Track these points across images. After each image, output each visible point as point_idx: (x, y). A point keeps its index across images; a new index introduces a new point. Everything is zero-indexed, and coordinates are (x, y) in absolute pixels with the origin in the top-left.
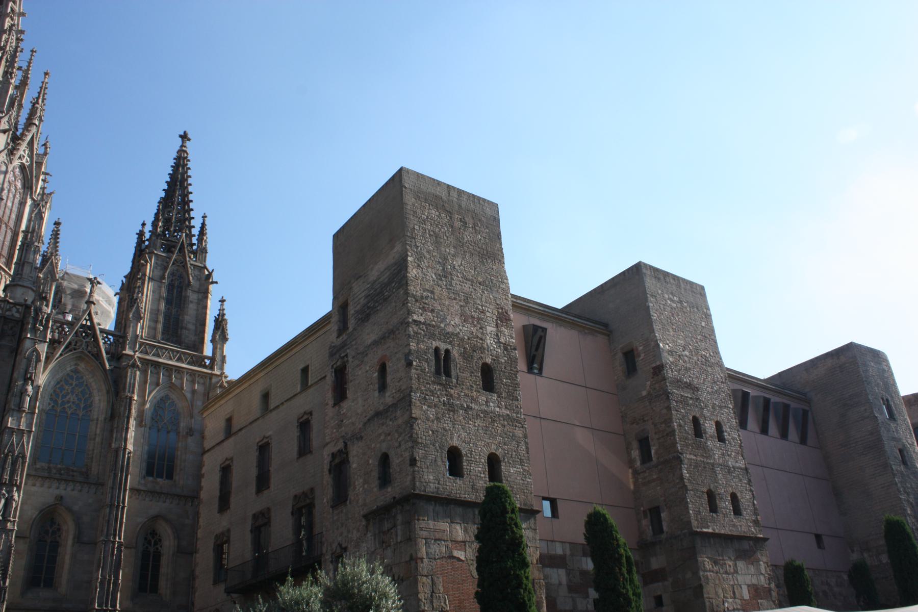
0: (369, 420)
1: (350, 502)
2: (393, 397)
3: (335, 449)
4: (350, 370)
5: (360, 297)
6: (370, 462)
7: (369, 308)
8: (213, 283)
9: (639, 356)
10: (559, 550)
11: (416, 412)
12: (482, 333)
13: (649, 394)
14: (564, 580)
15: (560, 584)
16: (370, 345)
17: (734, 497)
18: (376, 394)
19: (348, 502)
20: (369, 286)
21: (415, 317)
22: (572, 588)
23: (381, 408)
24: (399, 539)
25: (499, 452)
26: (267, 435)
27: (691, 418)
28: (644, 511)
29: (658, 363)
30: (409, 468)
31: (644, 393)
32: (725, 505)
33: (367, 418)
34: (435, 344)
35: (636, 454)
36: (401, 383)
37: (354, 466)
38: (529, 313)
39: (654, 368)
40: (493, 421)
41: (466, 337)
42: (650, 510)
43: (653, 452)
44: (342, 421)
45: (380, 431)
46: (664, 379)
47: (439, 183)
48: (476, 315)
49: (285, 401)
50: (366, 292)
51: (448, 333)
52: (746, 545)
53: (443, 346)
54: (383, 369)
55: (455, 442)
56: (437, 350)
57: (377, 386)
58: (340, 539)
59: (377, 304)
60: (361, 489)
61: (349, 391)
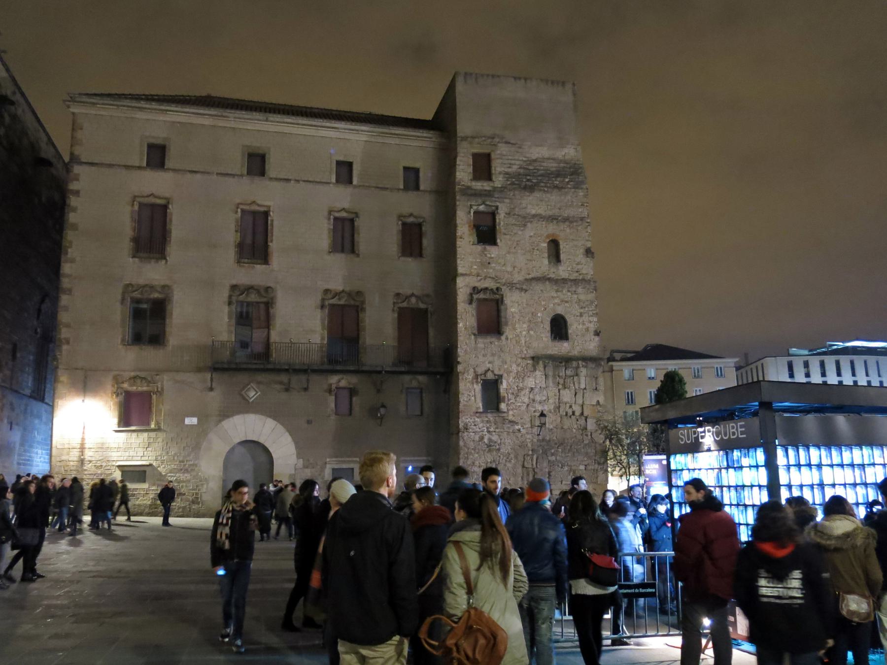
2: (570, 274)
3: (482, 285)
4: (502, 223)
5: (513, 162)
6: (539, 315)
7: (528, 180)
19: (503, 338)
20: (524, 159)
23: (552, 276)
24: (583, 386)
30: (593, 337)
33: (530, 276)
36: (580, 267)
44: (489, 263)
49: (304, 181)
50: (521, 163)
54: (554, 246)
59: (542, 184)
60: (524, 333)
61: (501, 241)
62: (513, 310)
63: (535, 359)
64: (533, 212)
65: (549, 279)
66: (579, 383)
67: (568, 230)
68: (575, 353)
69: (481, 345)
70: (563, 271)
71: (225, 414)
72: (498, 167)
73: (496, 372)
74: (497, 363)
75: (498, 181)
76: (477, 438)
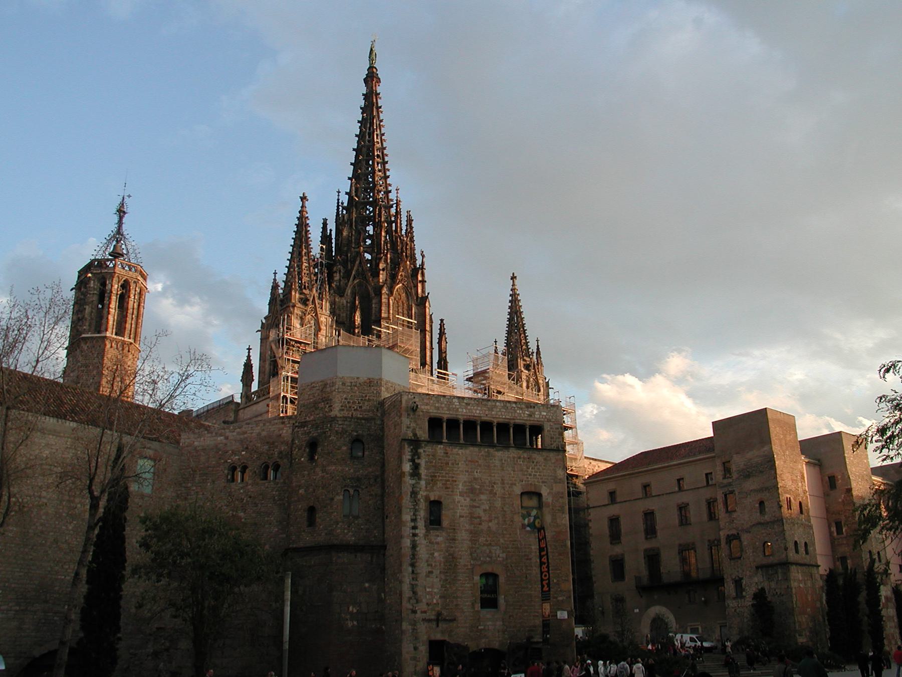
0: (754, 525)
1: (744, 559)
3: (730, 533)
7: (748, 472)
8: (551, 388)
9: (838, 481)
11: (785, 528)
13: (843, 501)
16: (751, 491)
17: (879, 553)
18: (758, 514)
19: (742, 558)
23: (762, 521)
25: (807, 542)
26: (651, 508)
28: (838, 558)
29: (849, 487)
31: (840, 500)
35: (834, 529)
37: (745, 543)
39: (847, 489)
42: (841, 558)
43: (844, 530)
45: (763, 531)
46: (852, 496)
54: (762, 503)
57: (758, 511)
58: (737, 573)
62: (745, 543)
63: (757, 568)
64: (751, 489)
65: (759, 524)
66: (778, 577)
67: (768, 494)
68: (776, 561)
69: (732, 564)
70: (767, 518)
71: (648, 607)
72: (734, 468)
73: (740, 576)
74: (740, 571)
75: (735, 475)
76: (733, 610)
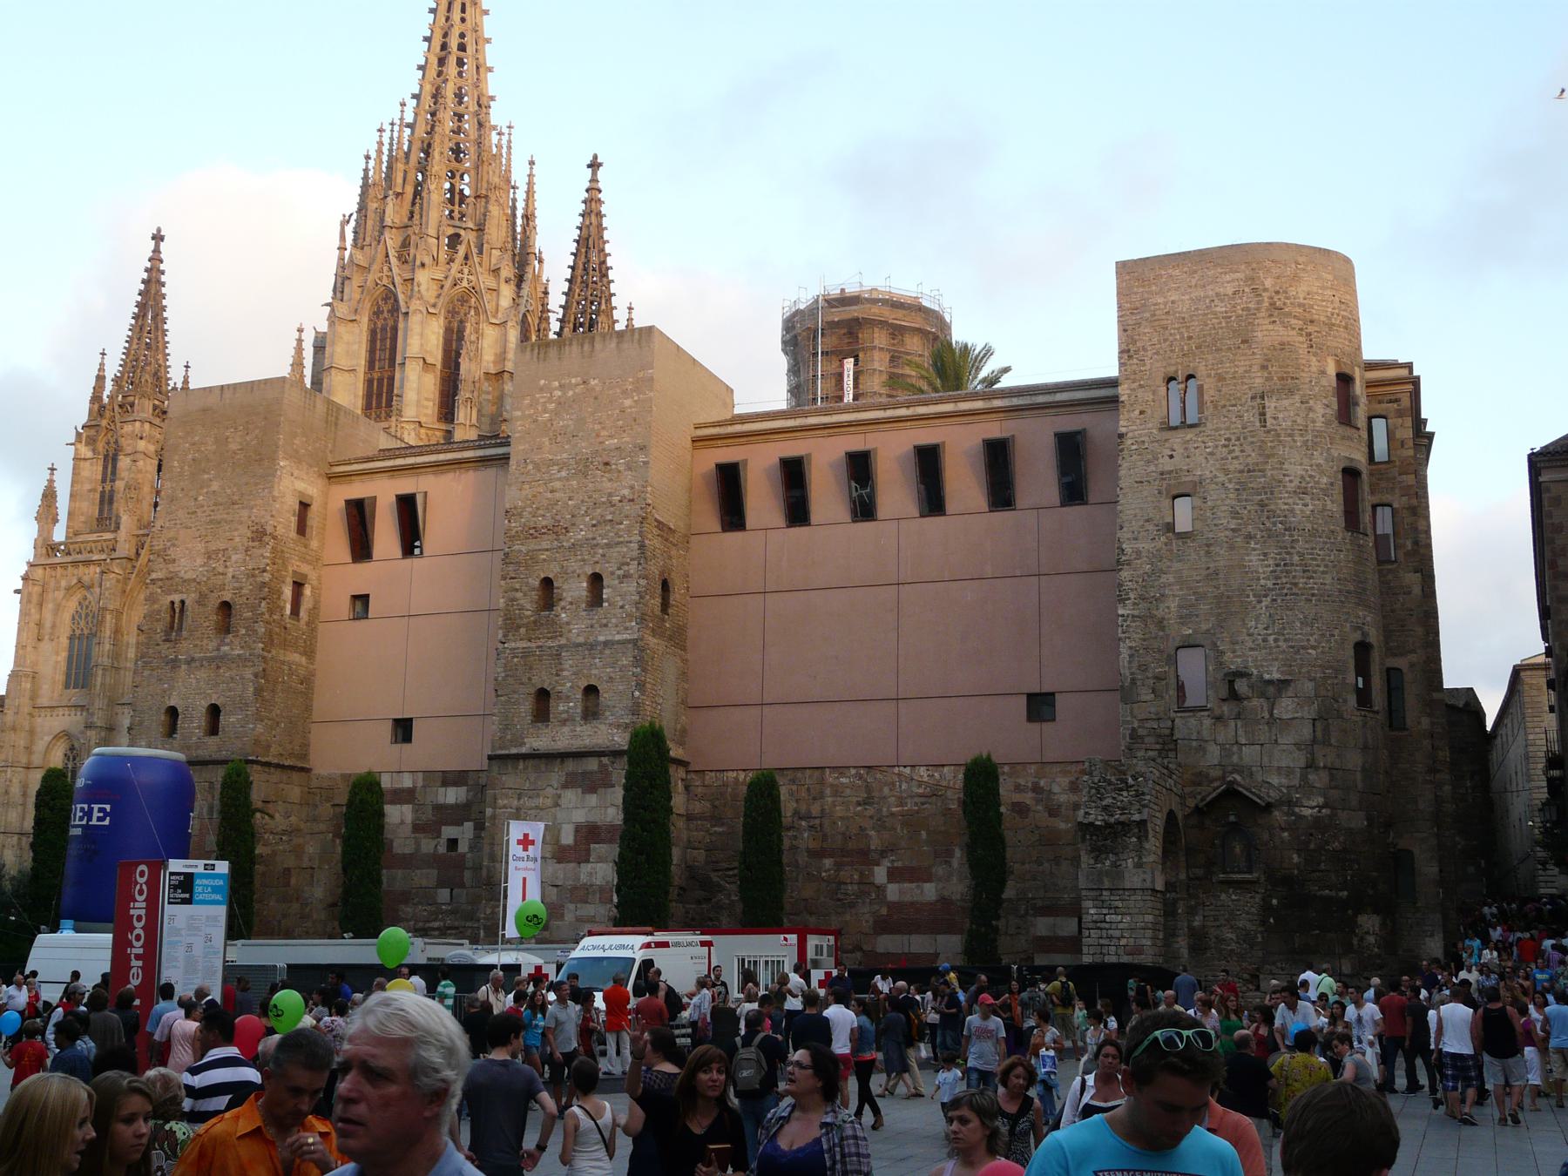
10: (407, 782)
12: (226, 567)
14: (409, 818)
15: (402, 822)
17: (591, 691)
21: (154, 576)
22: (417, 828)
27: (537, 583)
32: (568, 704)
34: (170, 598)
38: (418, 471)
40: (218, 667)
41: (205, 579)
47: (210, 389)
48: (222, 546)
51: (185, 581)
52: (592, 765)
53: (177, 598)
55: (172, 703)
56: (173, 603)
